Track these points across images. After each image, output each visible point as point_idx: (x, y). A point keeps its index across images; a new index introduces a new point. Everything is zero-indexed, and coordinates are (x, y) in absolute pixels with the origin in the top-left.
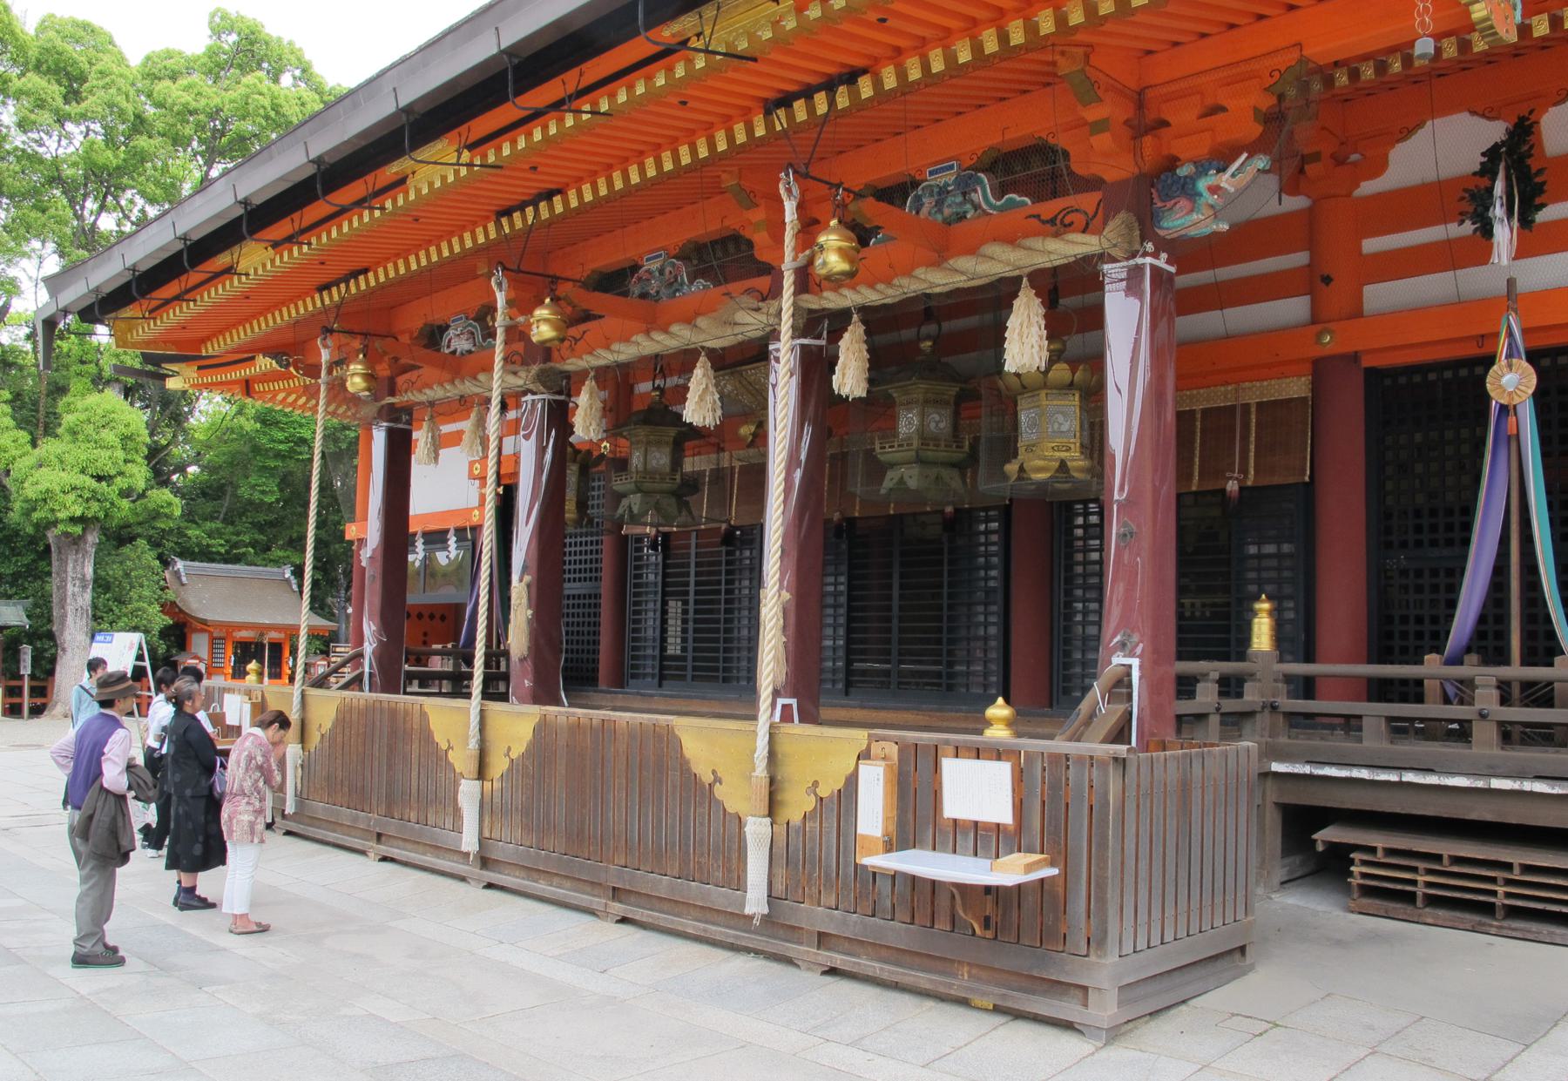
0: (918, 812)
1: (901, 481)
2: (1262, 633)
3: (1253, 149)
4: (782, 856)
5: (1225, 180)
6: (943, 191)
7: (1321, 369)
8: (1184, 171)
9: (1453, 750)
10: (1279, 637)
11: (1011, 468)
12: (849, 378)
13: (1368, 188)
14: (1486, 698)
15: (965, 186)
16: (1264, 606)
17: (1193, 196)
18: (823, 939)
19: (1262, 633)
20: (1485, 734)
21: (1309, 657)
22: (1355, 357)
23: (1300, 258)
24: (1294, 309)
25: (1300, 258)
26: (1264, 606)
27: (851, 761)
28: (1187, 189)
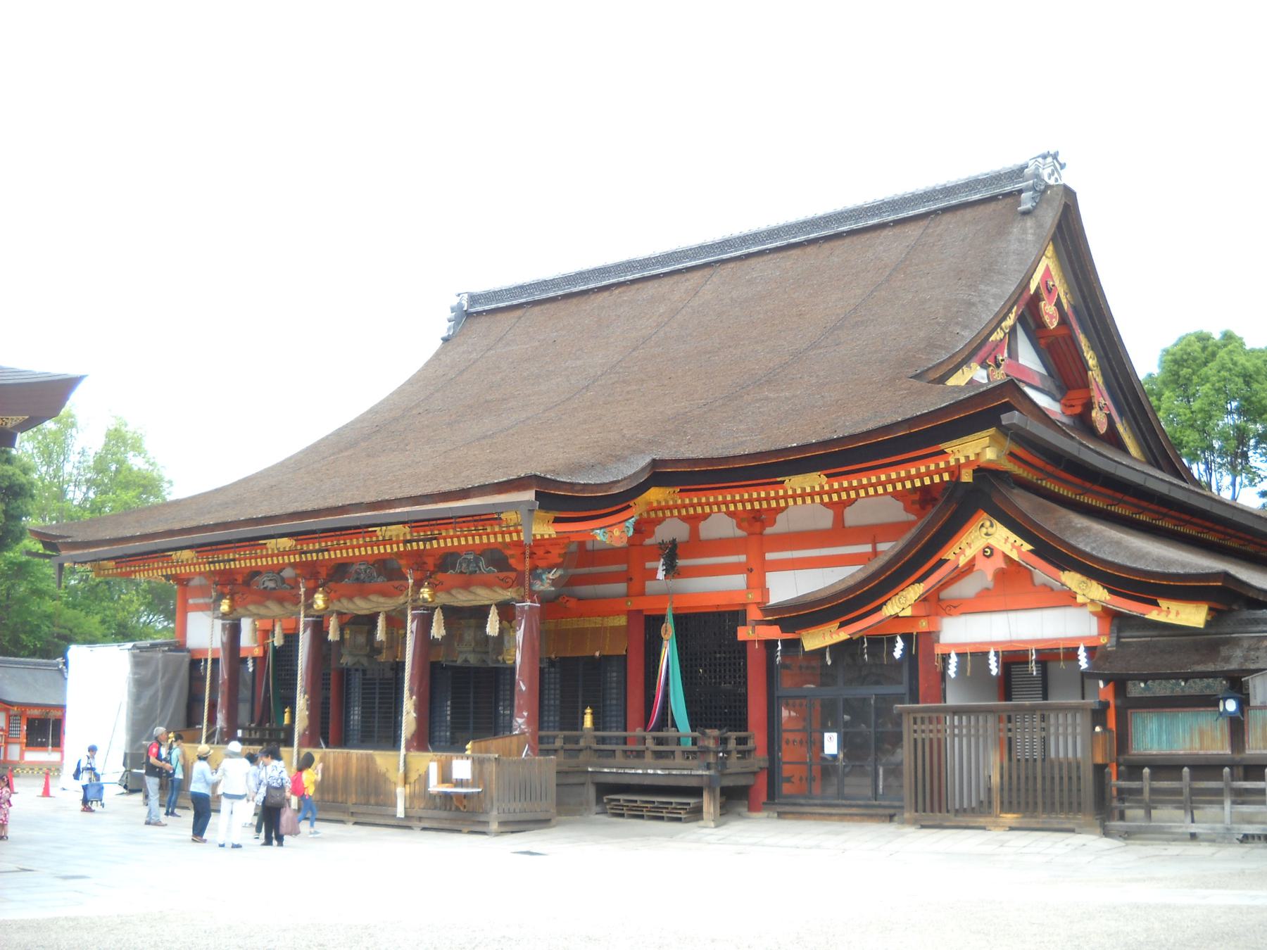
0: (445, 777)
1: (466, 661)
2: (588, 721)
3: (558, 566)
4: (411, 798)
5: (551, 576)
6: (469, 562)
7: (631, 614)
8: (539, 571)
9: (636, 761)
10: (595, 722)
11: (500, 658)
12: (438, 631)
13: (648, 542)
14: (650, 743)
15: (477, 560)
16: (588, 711)
17: (542, 580)
18: (420, 819)
19: (588, 721)
20: (648, 755)
21: (625, 730)
22: (640, 611)
23: (624, 567)
24: (621, 588)
25: (624, 567)
26: (588, 711)
27: (430, 764)
28: (539, 577)
